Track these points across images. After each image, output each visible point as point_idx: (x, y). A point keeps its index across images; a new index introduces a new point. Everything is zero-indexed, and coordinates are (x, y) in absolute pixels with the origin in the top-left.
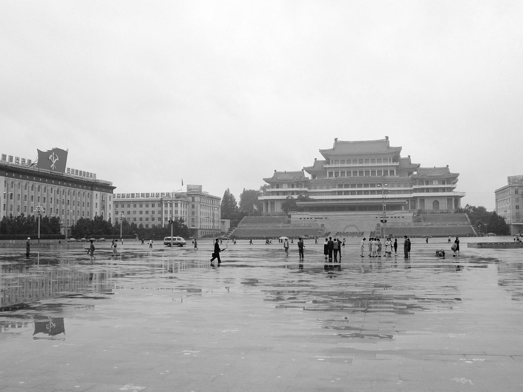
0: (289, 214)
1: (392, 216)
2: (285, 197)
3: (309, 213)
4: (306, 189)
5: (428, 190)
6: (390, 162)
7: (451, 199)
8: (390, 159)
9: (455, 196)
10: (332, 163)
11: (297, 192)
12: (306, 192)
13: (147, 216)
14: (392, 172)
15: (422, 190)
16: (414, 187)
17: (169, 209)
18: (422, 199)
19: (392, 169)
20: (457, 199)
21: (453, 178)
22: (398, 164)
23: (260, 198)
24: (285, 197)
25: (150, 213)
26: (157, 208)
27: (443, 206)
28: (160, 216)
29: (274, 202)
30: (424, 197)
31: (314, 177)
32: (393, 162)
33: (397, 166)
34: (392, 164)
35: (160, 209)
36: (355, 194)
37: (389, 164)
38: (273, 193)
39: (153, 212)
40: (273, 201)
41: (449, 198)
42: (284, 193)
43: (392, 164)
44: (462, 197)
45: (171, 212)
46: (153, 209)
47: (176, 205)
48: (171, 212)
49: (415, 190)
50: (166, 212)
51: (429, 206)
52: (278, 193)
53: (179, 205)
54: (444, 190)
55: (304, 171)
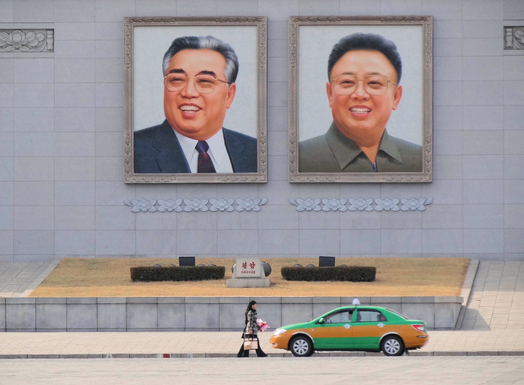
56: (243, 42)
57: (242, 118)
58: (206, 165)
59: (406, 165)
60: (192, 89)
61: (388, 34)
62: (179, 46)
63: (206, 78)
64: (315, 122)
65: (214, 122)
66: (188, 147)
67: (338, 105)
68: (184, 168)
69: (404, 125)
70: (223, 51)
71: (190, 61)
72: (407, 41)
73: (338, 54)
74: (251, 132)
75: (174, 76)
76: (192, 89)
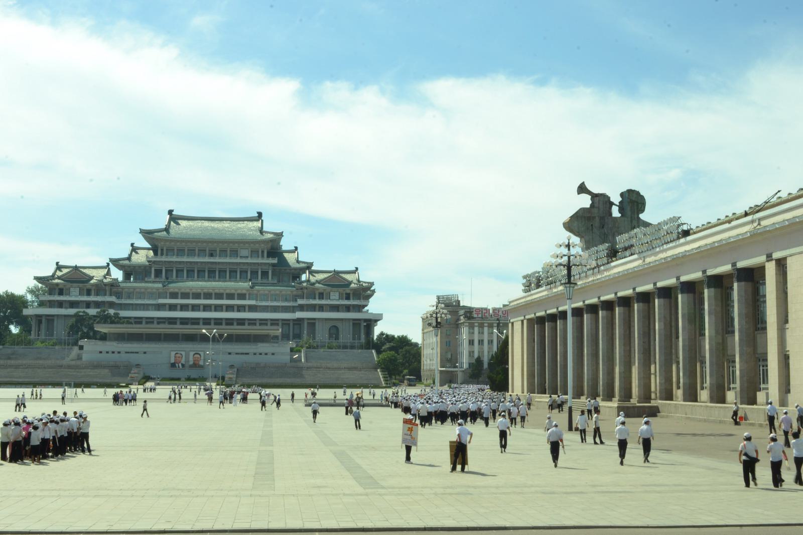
0: (80, 343)
1: (255, 351)
2: (72, 311)
3: (115, 344)
4: (113, 299)
5: (321, 308)
6: (263, 256)
7: (360, 324)
8: (263, 252)
9: (365, 320)
10: (162, 254)
11: (97, 304)
12: (112, 305)
14: (265, 274)
15: (313, 308)
16: (300, 302)
18: (312, 323)
19: (265, 268)
20: (370, 323)
21: (365, 292)
22: (275, 261)
23: (26, 312)
24: (72, 311)
27: (346, 336)
29: (53, 320)
30: (314, 319)
31: (127, 276)
32: (268, 256)
33: (274, 265)
34: (266, 261)
36: (199, 310)
37: (260, 261)
38: (51, 304)
40: (50, 319)
41: (356, 323)
42: (73, 304)
43: (266, 261)
44: (379, 320)
49: (302, 308)
51: (322, 334)
52: (60, 304)
54: (348, 309)
55: (111, 266)
56: (183, 353)
57: (183, 361)
58: (179, 367)
59: (202, 367)
60: (178, 358)
61: (200, 353)
62: (176, 354)
63: (179, 357)
64: (191, 363)
65: (180, 362)
66: (177, 365)
67: (194, 361)
68: (176, 367)
69: (201, 363)
70: (181, 354)
71: (177, 355)
72: (202, 354)
73: (194, 355)
74: (184, 363)
75: (175, 357)
76: (178, 358)
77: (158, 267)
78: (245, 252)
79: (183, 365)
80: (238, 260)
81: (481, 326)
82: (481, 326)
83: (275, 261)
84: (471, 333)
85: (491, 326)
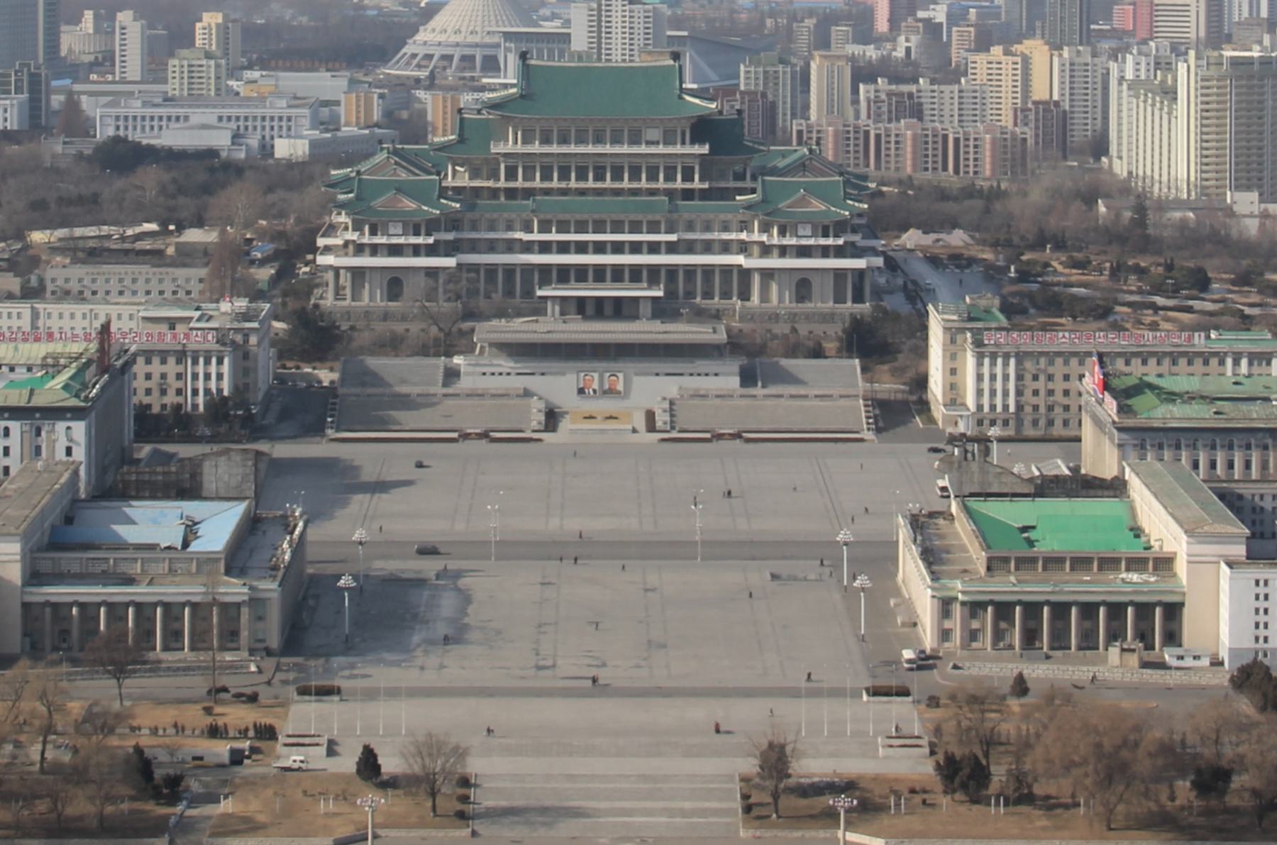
6: (683, 143)
8: (683, 134)
13: (148, 384)
17: (201, 369)
22: (705, 149)
25: (156, 377)
26: (171, 367)
28: (180, 384)
32: (693, 142)
35: (180, 369)
37: (678, 149)
39: (163, 376)
45: (207, 377)
46: (164, 369)
47: (220, 362)
48: (207, 377)
50: (195, 377)
53: (226, 361)
69: (620, 387)
77: (511, 162)
78: (653, 134)
79: (595, 391)
80: (643, 149)
81: (993, 357)
82: (993, 357)
83: (705, 149)
84: (980, 364)
85: (1006, 357)
